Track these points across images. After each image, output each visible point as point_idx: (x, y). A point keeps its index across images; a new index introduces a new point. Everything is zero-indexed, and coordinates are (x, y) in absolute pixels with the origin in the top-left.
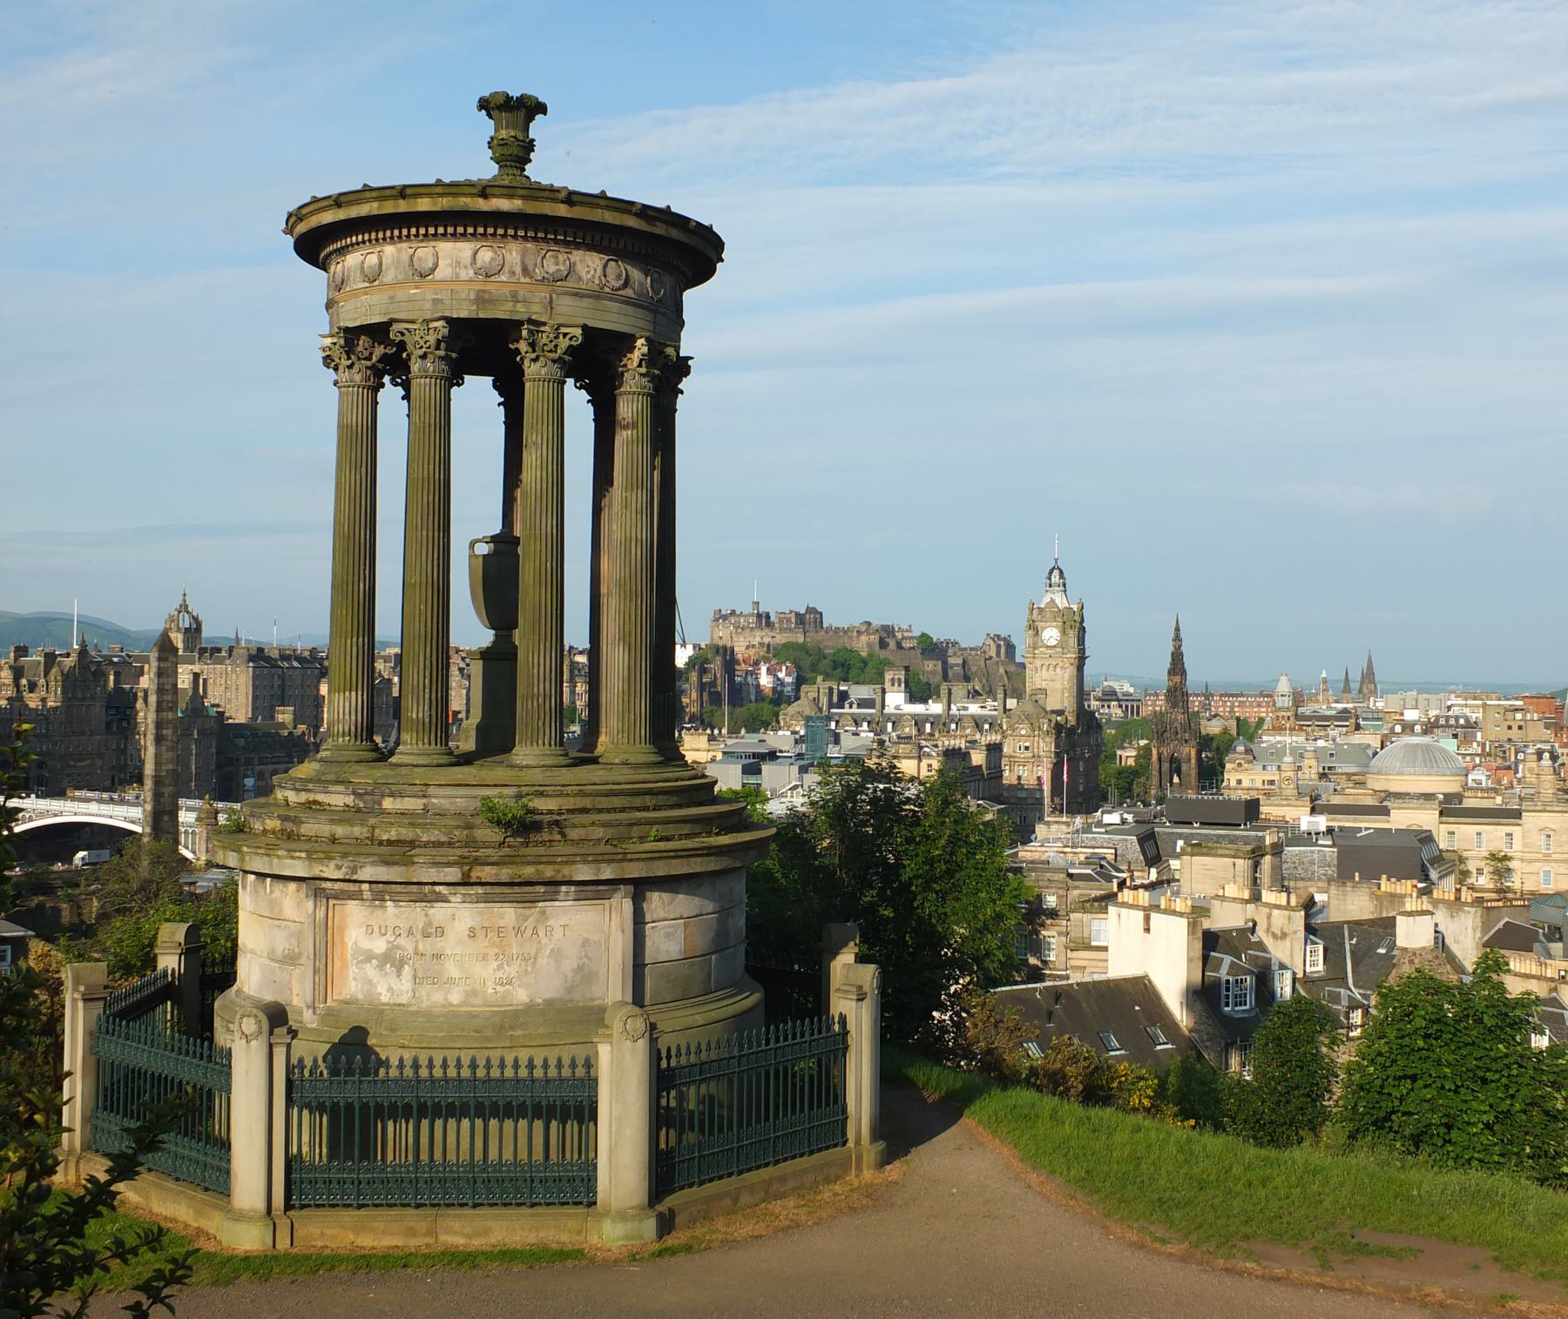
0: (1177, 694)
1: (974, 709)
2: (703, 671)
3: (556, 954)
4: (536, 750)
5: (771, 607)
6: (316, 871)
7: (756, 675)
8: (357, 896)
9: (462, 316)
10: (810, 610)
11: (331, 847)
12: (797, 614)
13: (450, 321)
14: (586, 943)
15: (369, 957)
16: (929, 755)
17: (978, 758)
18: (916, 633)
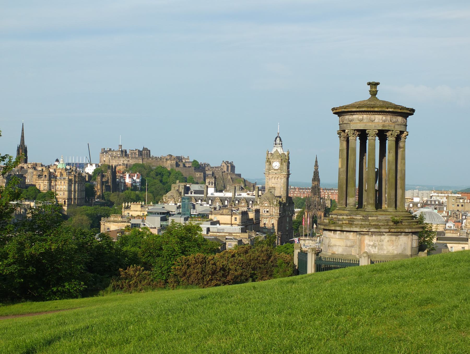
0: (316, 189)
1: (244, 195)
2: (103, 176)
3: (401, 245)
4: (392, 209)
5: (128, 147)
6: (361, 230)
7: (124, 178)
8: (368, 235)
9: (380, 129)
10: (145, 149)
11: (361, 226)
12: (139, 151)
13: (379, 130)
14: (405, 243)
15: (369, 245)
16: (235, 214)
17: (251, 215)
18: (191, 160)
